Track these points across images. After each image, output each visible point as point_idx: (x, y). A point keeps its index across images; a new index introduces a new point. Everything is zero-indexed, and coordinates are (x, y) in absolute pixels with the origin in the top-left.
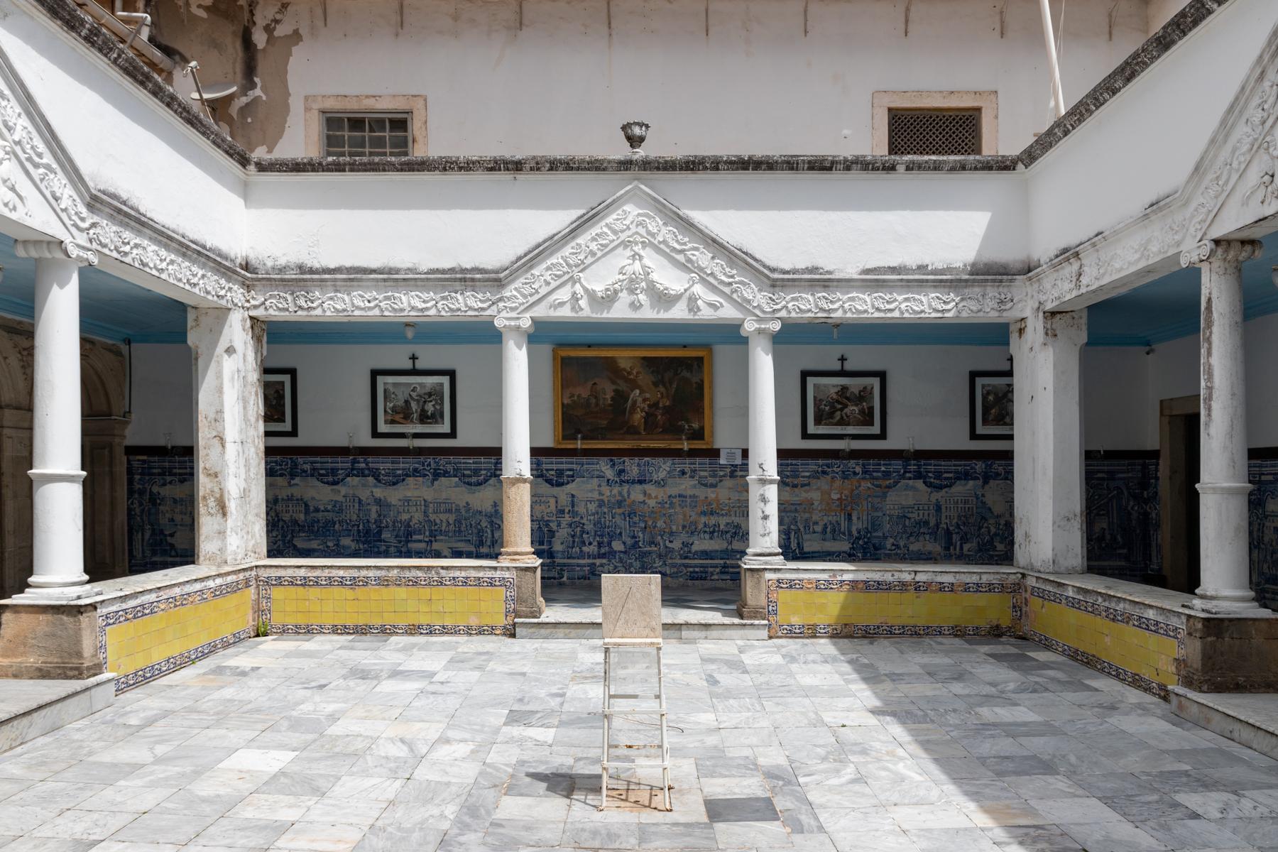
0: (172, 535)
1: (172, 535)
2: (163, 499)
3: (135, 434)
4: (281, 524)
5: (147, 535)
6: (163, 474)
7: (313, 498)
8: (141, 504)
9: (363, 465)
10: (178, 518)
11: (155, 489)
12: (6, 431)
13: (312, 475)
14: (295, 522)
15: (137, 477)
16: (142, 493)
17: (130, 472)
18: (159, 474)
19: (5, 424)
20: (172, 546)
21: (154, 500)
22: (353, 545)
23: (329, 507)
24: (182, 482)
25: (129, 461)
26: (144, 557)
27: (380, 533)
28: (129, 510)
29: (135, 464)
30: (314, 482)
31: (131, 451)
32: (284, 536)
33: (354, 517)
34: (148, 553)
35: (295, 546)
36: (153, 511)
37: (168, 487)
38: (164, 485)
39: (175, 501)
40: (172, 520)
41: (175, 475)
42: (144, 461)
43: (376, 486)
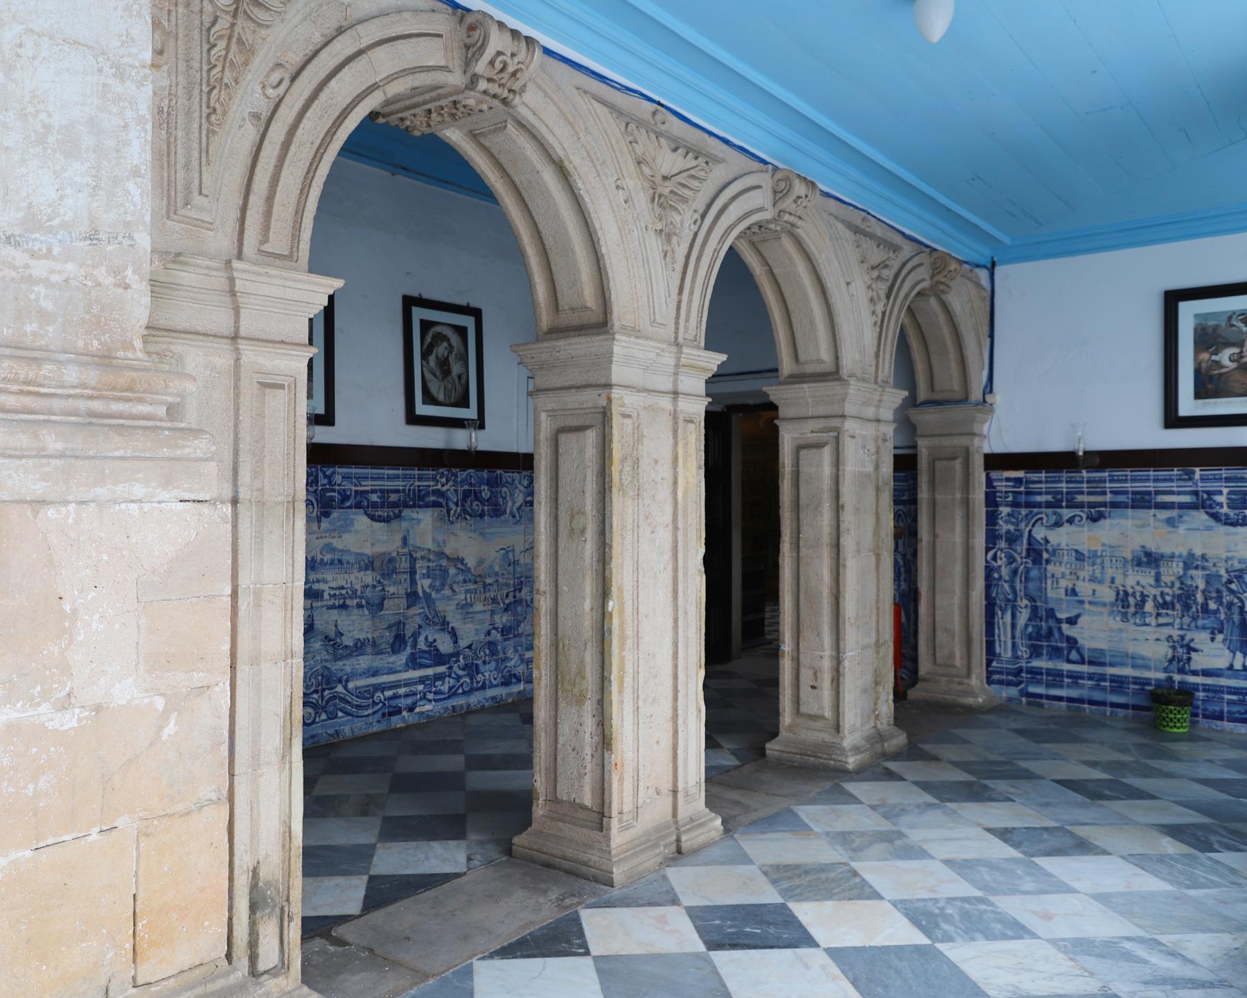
0: (1072, 621)
1: (1072, 621)
2: (1054, 553)
3: (1012, 426)
6: (1055, 505)
8: (1011, 560)
10: (1084, 588)
11: (1039, 533)
12: (850, 425)
15: (1005, 510)
16: (1012, 539)
17: (991, 500)
18: (1048, 505)
19: (849, 409)
20: (1072, 642)
21: (1035, 553)
24: (1094, 519)
25: (989, 482)
26: (1016, 657)
28: (989, 570)
29: (1001, 486)
31: (996, 462)
34: (1023, 651)
36: (1034, 573)
37: (1067, 528)
38: (1058, 524)
39: (1079, 556)
40: (1074, 592)
41: (1080, 506)
42: (1018, 481)
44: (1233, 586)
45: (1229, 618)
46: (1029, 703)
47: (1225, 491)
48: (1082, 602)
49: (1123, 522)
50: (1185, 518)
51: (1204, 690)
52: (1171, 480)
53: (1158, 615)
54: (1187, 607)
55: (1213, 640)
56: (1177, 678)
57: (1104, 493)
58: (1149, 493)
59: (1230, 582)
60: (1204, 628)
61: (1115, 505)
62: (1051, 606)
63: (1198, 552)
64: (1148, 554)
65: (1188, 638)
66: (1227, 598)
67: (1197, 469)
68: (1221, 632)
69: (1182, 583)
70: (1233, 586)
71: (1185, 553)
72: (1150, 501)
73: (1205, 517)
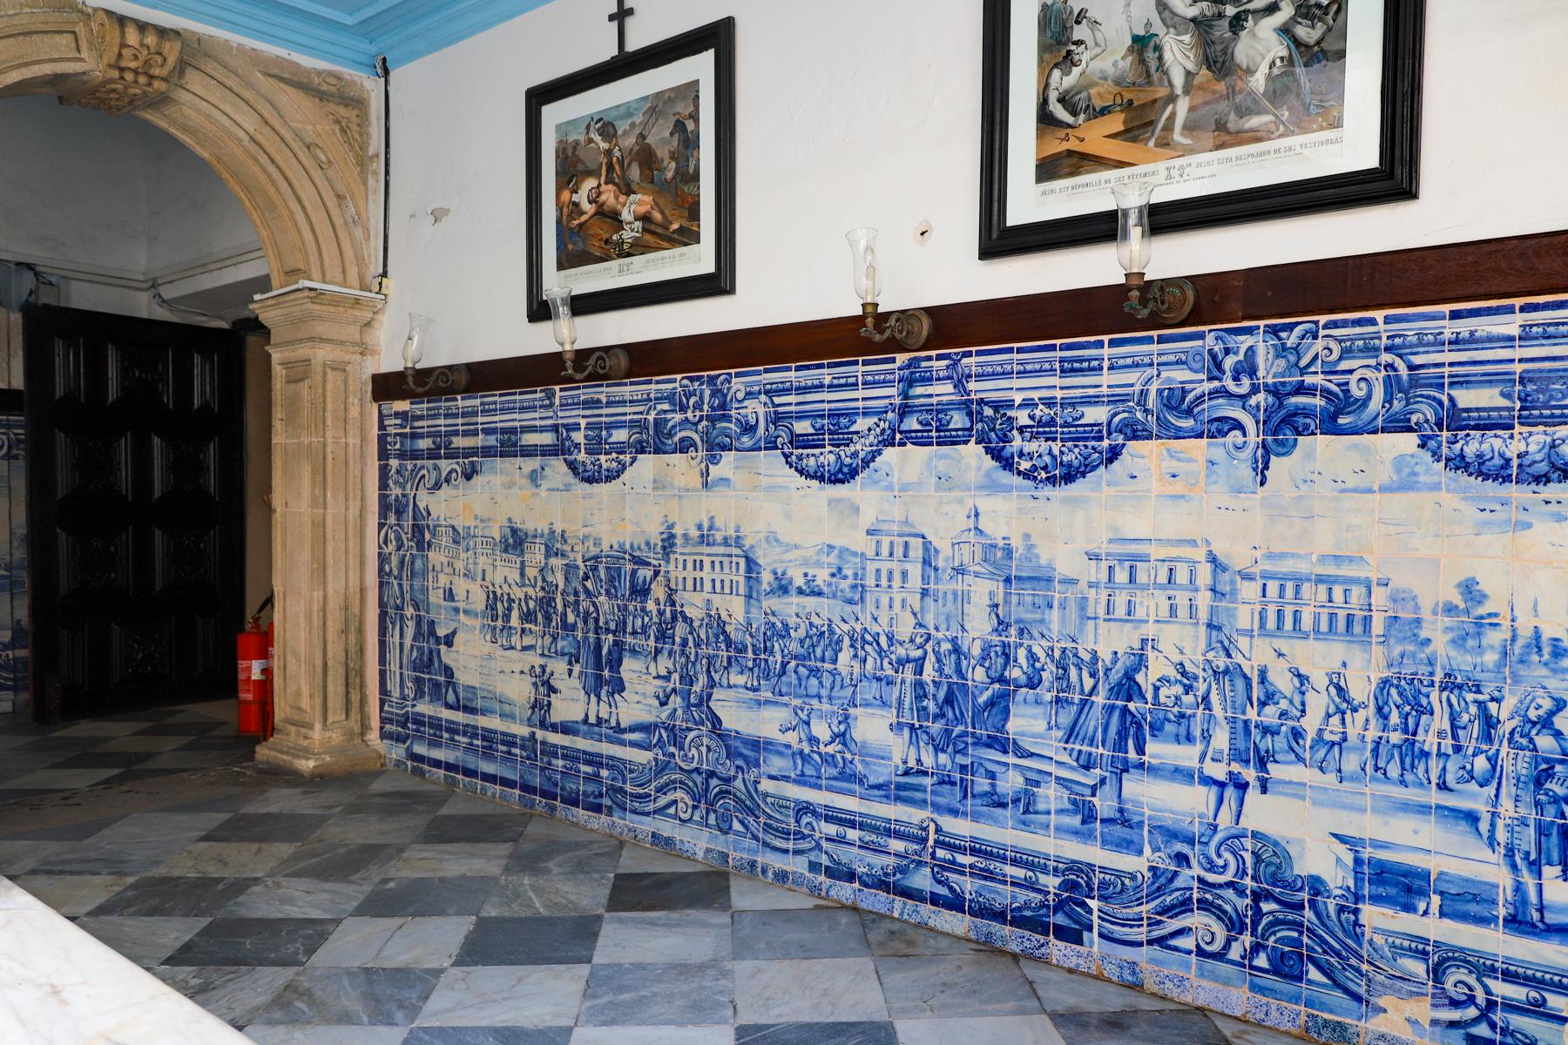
4: (680, 630)
5: (410, 632)
7: (772, 539)
9: (944, 391)
13: (772, 445)
14: (718, 626)
22: (899, 749)
23: (822, 577)
27: (1000, 705)
30: (771, 464)
31: (387, 386)
32: (687, 679)
33: (905, 628)
35: (716, 721)
43: (992, 487)
44: (589, 584)
45: (586, 638)
46: (414, 769)
47: (583, 422)
48: (457, 610)
49: (492, 478)
50: (547, 471)
51: (565, 757)
52: (533, 408)
53: (523, 631)
54: (548, 618)
55: (570, 673)
56: (540, 734)
57: (475, 433)
58: (513, 431)
59: (586, 577)
60: (563, 654)
61: (487, 452)
62: (432, 616)
63: (558, 529)
64: (514, 531)
65: (548, 670)
66: (585, 604)
67: (557, 388)
68: (577, 661)
69: (544, 580)
70: (589, 584)
71: (547, 531)
72: (515, 445)
73: (564, 468)
